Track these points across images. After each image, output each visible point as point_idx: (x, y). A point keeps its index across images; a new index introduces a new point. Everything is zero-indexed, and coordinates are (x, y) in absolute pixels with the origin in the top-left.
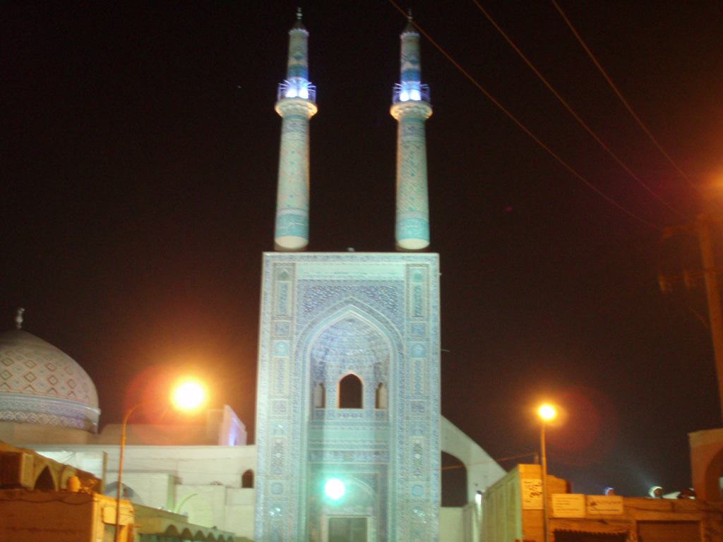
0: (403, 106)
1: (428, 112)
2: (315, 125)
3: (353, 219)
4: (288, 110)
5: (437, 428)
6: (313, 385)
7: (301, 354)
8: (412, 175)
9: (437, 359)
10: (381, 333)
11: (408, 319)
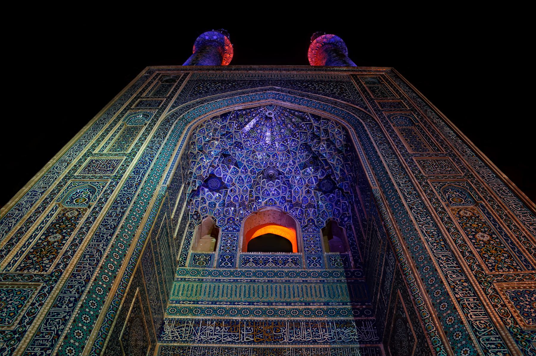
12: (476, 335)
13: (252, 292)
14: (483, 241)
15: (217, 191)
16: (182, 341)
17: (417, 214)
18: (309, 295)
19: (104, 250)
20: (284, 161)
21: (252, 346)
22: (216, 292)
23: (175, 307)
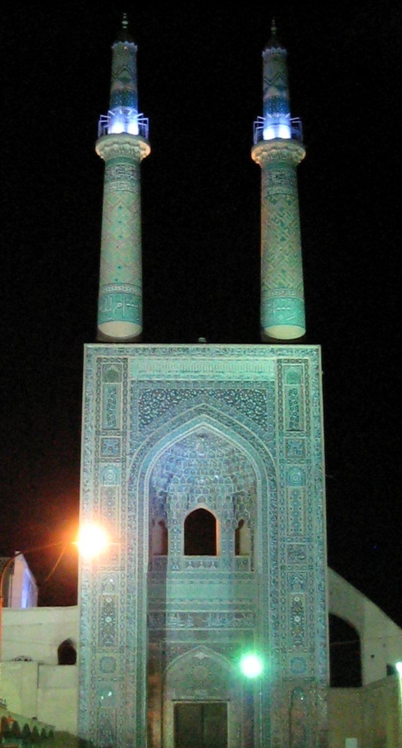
0: (267, 146)
1: (300, 154)
2: (147, 171)
3: (200, 297)
4: (113, 150)
5: (324, 580)
6: (152, 523)
7: (137, 481)
8: (283, 239)
9: (322, 489)
10: (245, 452)
11: (281, 434)
20: (212, 468)
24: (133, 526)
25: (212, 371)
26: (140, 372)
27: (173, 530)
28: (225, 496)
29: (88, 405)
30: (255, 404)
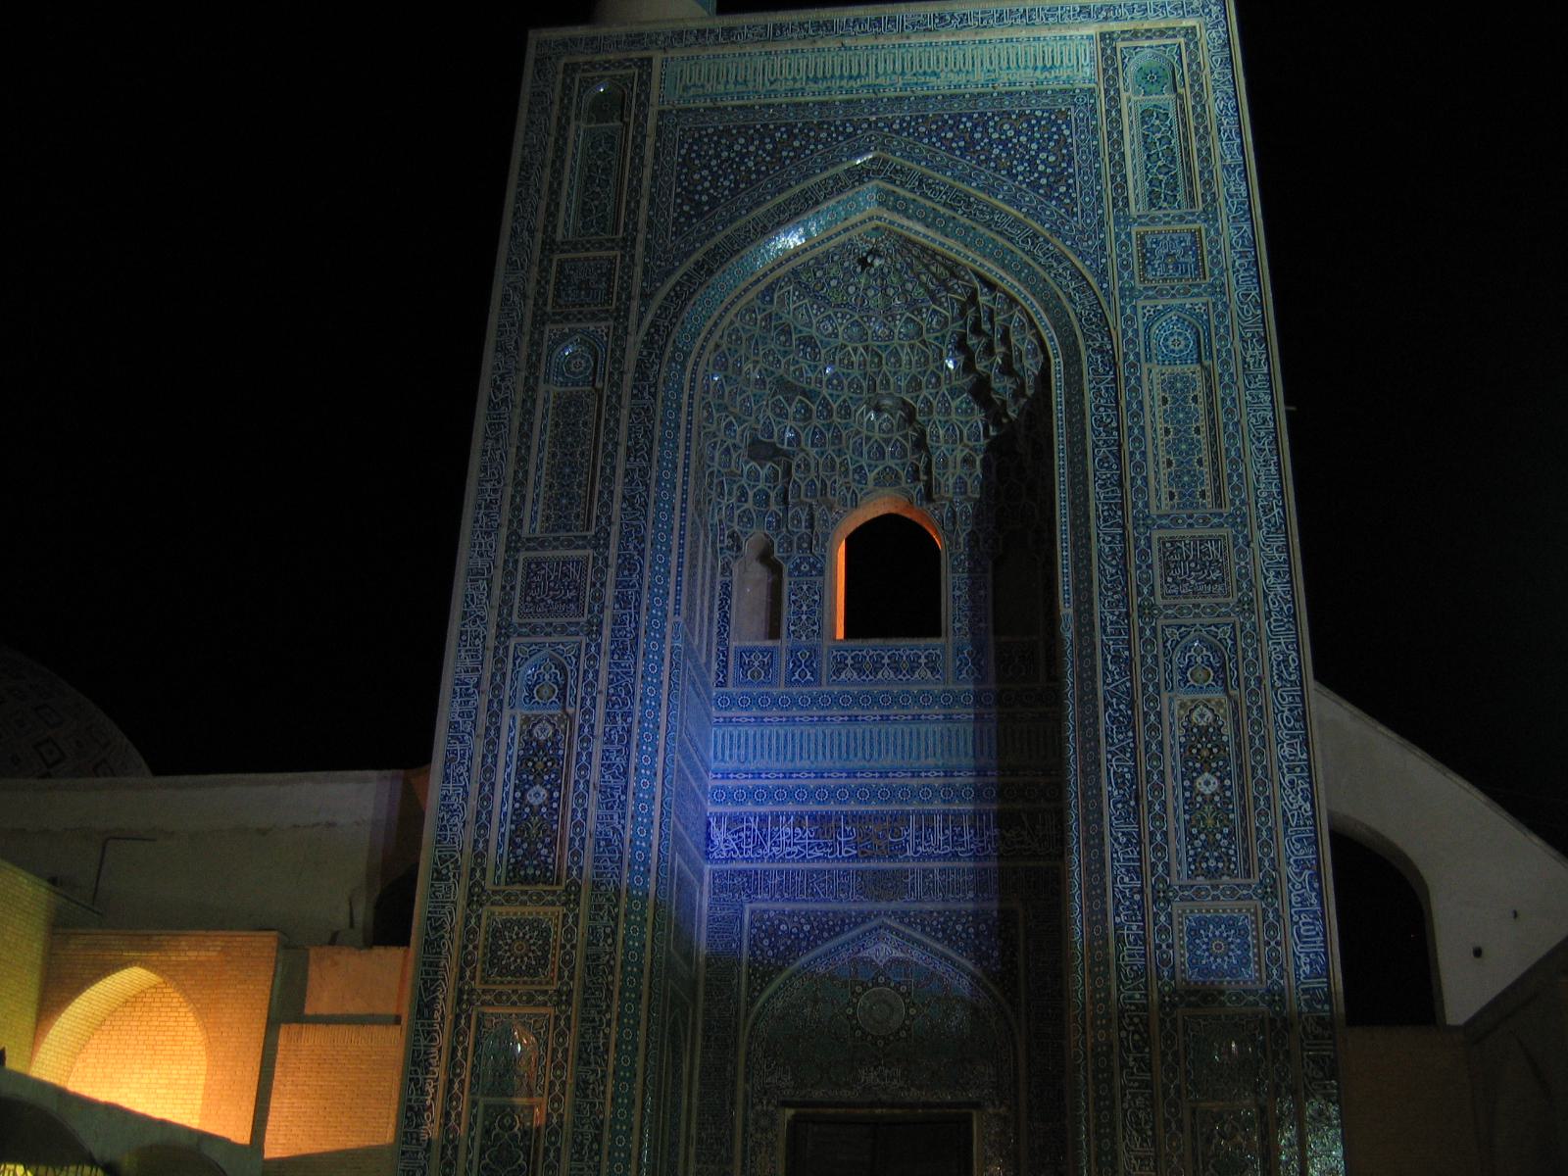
11: (1122, 220)
12: (1119, 989)
13: (852, 745)
14: (1203, 795)
15: (770, 458)
16: (744, 858)
17: (1113, 723)
18: (954, 752)
19: (623, 828)
20: (914, 371)
21: (855, 865)
22: (790, 747)
23: (722, 787)
24: (638, 500)
25: (903, 73)
26: (686, 88)
27: (797, 567)
28: (959, 457)
29: (529, 179)
30: (1034, 146)
